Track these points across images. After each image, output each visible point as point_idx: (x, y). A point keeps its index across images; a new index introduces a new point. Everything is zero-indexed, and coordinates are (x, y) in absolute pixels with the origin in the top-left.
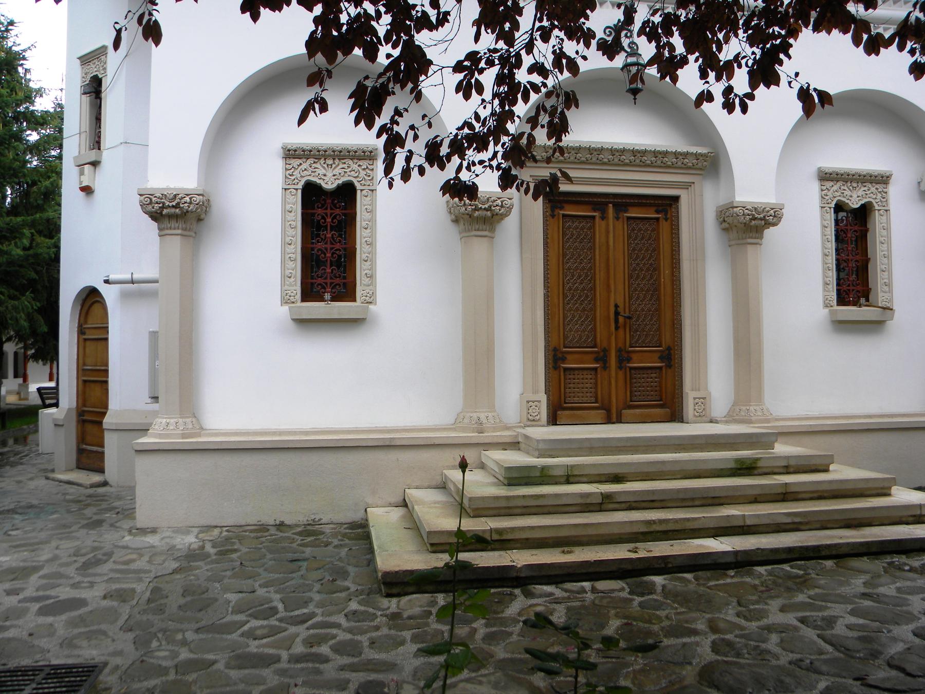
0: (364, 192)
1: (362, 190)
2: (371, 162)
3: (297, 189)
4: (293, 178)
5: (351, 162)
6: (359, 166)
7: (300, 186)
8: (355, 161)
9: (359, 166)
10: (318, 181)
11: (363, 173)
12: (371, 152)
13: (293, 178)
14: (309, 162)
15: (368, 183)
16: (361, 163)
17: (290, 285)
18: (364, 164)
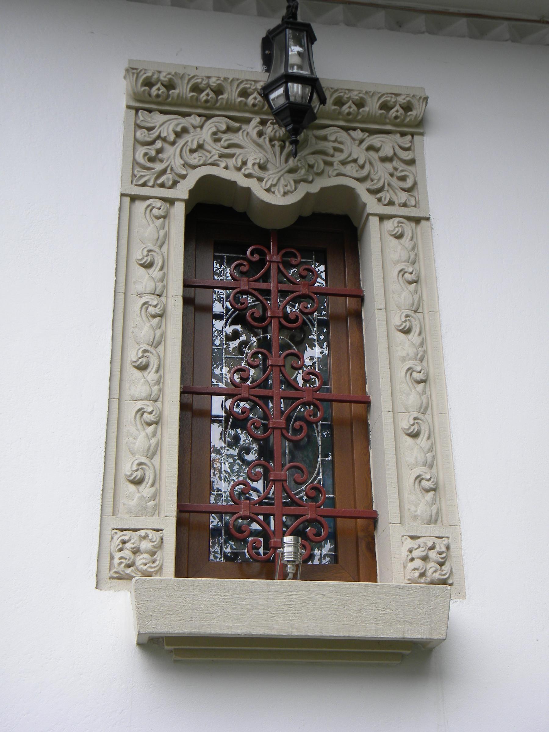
0: (389, 225)
1: (382, 218)
2: (406, 141)
3: (171, 202)
4: (159, 167)
5: (343, 135)
6: (370, 148)
7: (183, 191)
8: (358, 134)
9: (370, 148)
10: (243, 182)
11: (382, 172)
12: (407, 108)
13: (159, 167)
14: (210, 127)
15: (403, 197)
16: (376, 140)
17: (142, 511)
18: (388, 144)
